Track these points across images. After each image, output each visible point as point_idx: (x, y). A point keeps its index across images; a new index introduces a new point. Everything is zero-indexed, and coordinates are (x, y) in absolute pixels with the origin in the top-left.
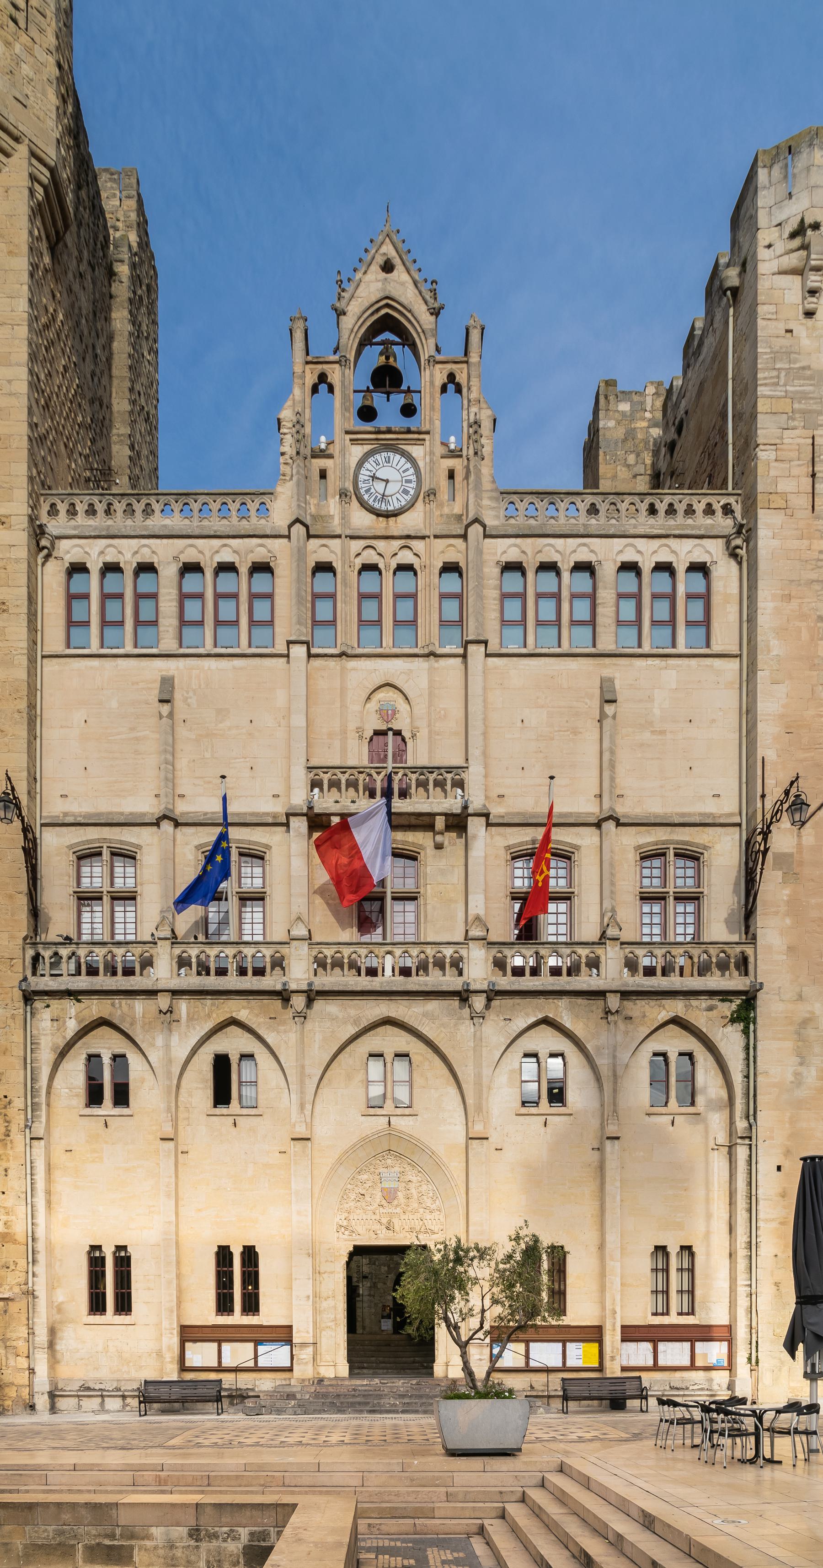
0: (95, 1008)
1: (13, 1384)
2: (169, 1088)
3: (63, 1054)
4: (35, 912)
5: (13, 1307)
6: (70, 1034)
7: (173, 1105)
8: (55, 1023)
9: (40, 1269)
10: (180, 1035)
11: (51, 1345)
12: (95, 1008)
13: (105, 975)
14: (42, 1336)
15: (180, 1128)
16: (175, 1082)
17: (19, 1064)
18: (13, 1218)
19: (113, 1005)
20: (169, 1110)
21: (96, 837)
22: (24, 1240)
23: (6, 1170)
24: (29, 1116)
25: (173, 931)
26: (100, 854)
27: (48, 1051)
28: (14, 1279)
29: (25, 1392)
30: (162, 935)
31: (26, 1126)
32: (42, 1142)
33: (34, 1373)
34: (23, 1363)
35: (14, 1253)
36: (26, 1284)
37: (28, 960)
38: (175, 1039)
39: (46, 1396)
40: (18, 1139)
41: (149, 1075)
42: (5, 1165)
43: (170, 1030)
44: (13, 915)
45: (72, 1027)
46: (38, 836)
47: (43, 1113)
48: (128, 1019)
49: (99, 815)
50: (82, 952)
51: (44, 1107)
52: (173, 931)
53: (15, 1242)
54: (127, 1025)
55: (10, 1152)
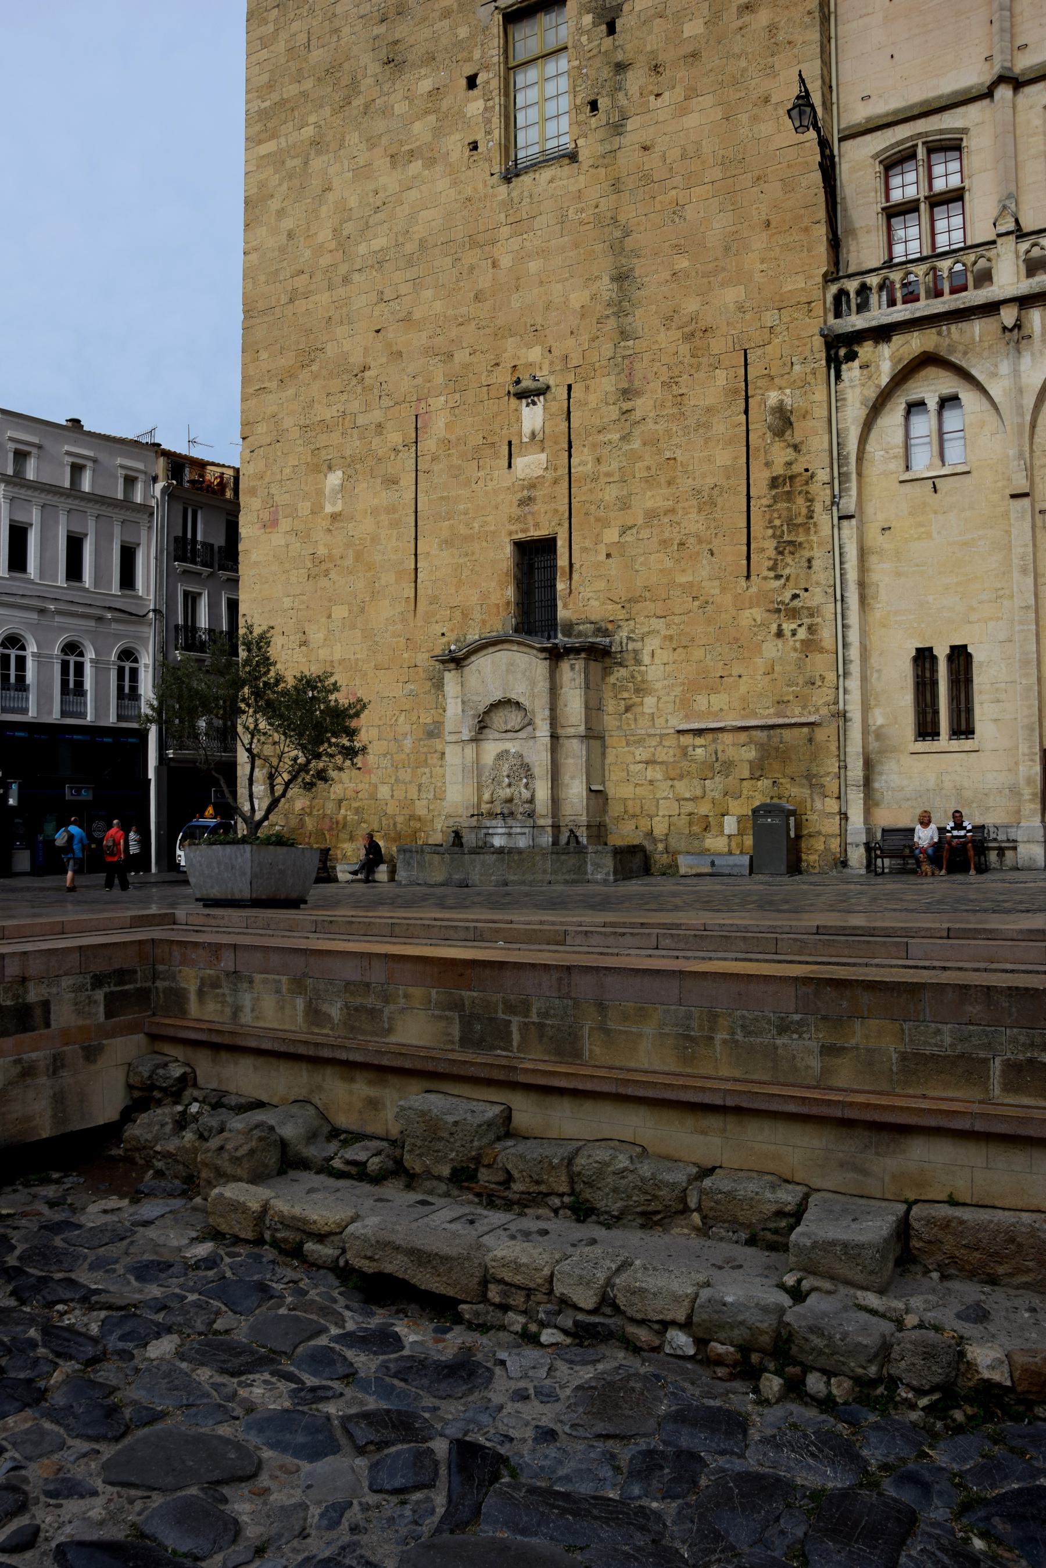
0: (915, 343)
1: (819, 833)
2: (1021, 426)
3: (877, 408)
4: (835, 244)
5: (820, 735)
6: (885, 380)
7: (1027, 448)
8: (865, 372)
9: (854, 684)
10: (1033, 354)
11: (867, 782)
12: (915, 343)
13: (927, 298)
14: (856, 771)
15: (1037, 479)
16: (1028, 418)
17: (821, 426)
18: (819, 620)
19: (939, 334)
20: (1021, 455)
21: (908, 134)
22: (832, 648)
23: (809, 561)
24: (836, 492)
25: (1017, 221)
26: (913, 156)
27: (858, 405)
28: (821, 697)
29: (835, 844)
30: (1002, 229)
31: (833, 503)
32: (854, 521)
33: (847, 819)
34: (832, 806)
35: (820, 664)
36: (836, 703)
37: (829, 299)
38: (1026, 360)
39: (862, 850)
40: (824, 520)
41: (991, 417)
42: (807, 554)
43: (1019, 352)
44: (809, 251)
45: (885, 372)
46: (836, 152)
47: (853, 484)
48: (961, 347)
49: (912, 107)
50: (896, 276)
51: (854, 477)
52: (1017, 221)
53: (821, 650)
54: (960, 355)
55: (814, 538)
